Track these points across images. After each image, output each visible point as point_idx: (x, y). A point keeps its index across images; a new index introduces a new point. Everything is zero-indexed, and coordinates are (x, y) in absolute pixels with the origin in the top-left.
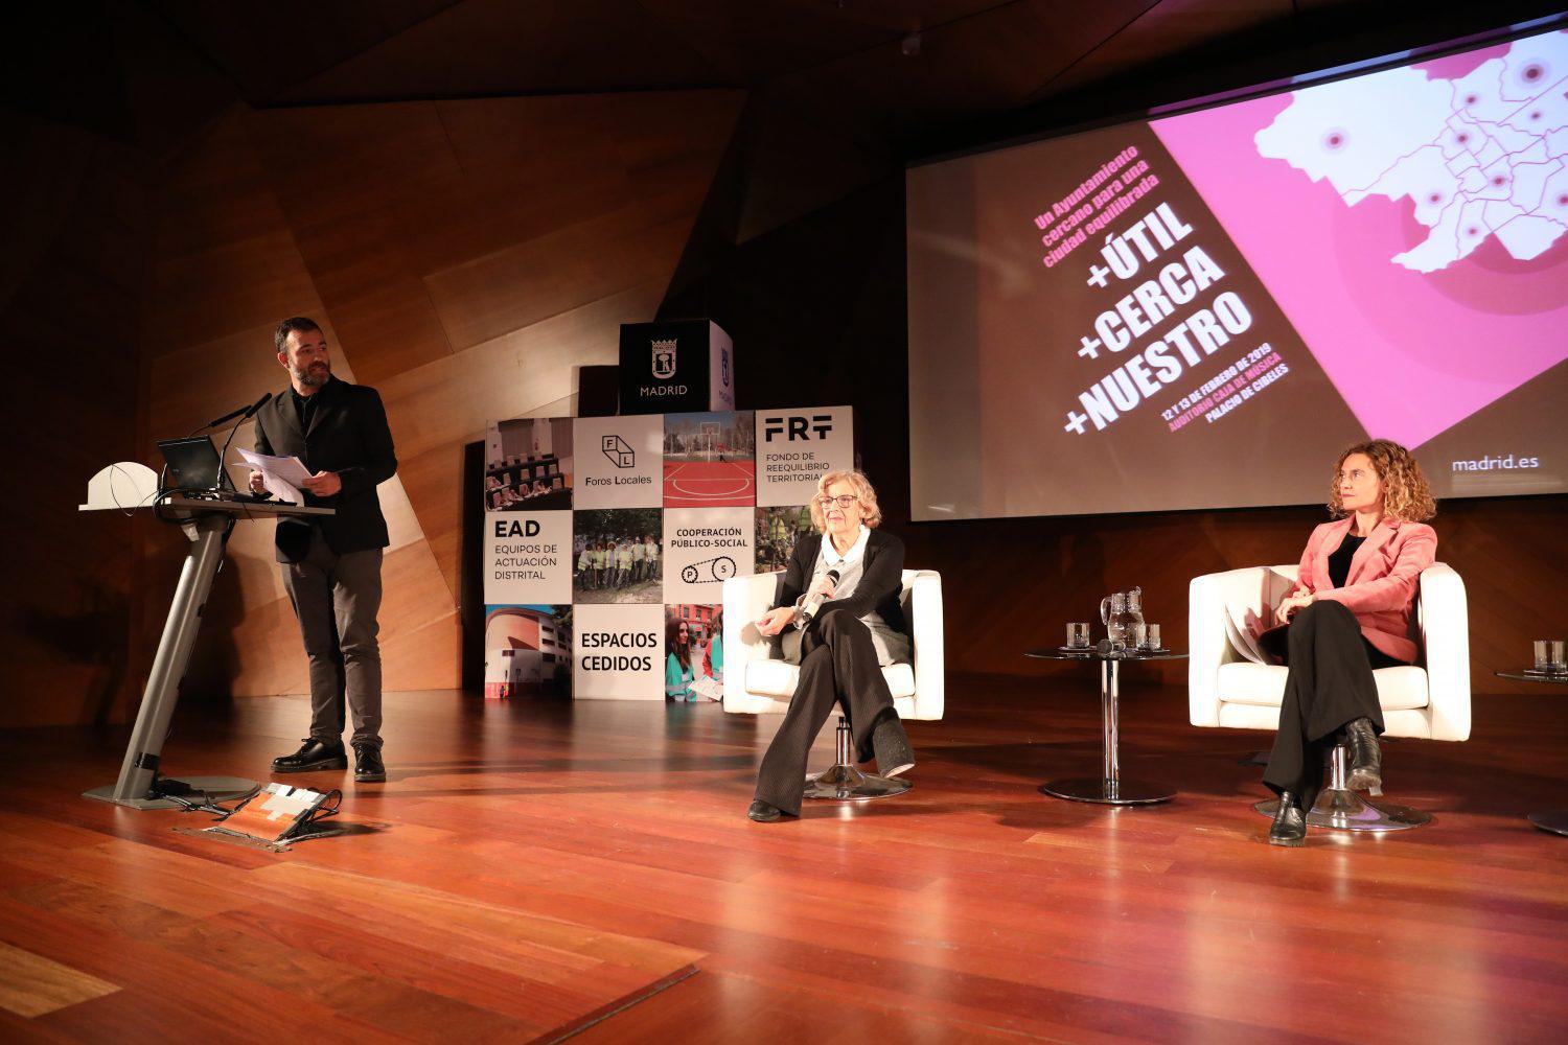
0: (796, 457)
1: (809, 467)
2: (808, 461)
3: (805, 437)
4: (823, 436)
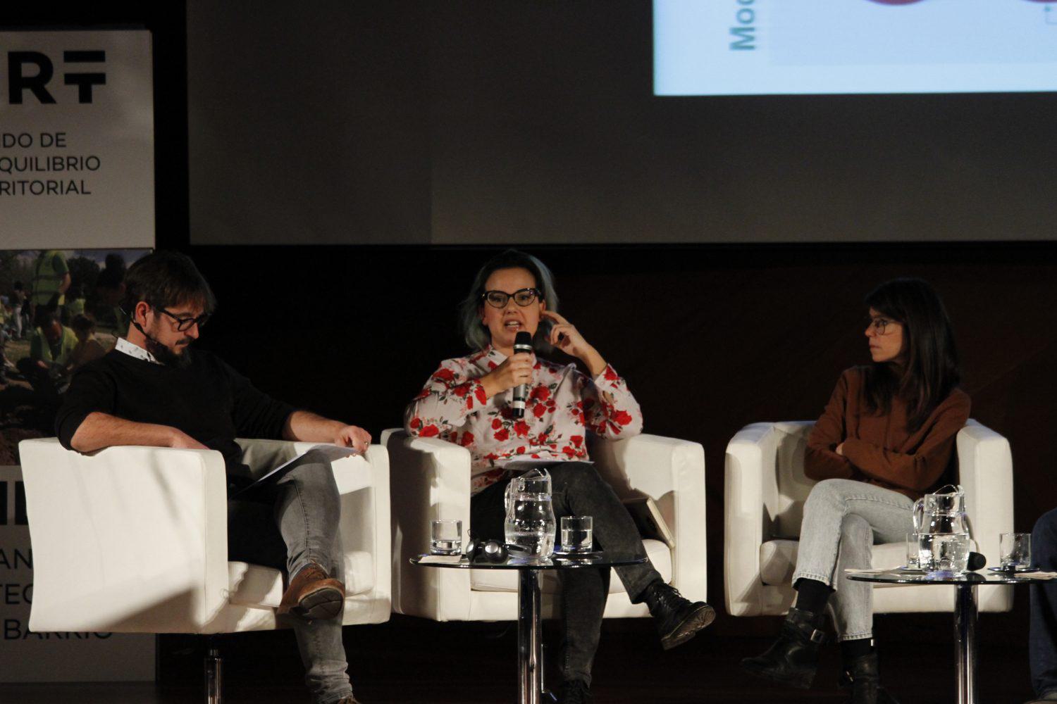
0: (25, 140)
1: (55, 164)
2: (53, 151)
3: (46, 98)
4: (85, 97)
